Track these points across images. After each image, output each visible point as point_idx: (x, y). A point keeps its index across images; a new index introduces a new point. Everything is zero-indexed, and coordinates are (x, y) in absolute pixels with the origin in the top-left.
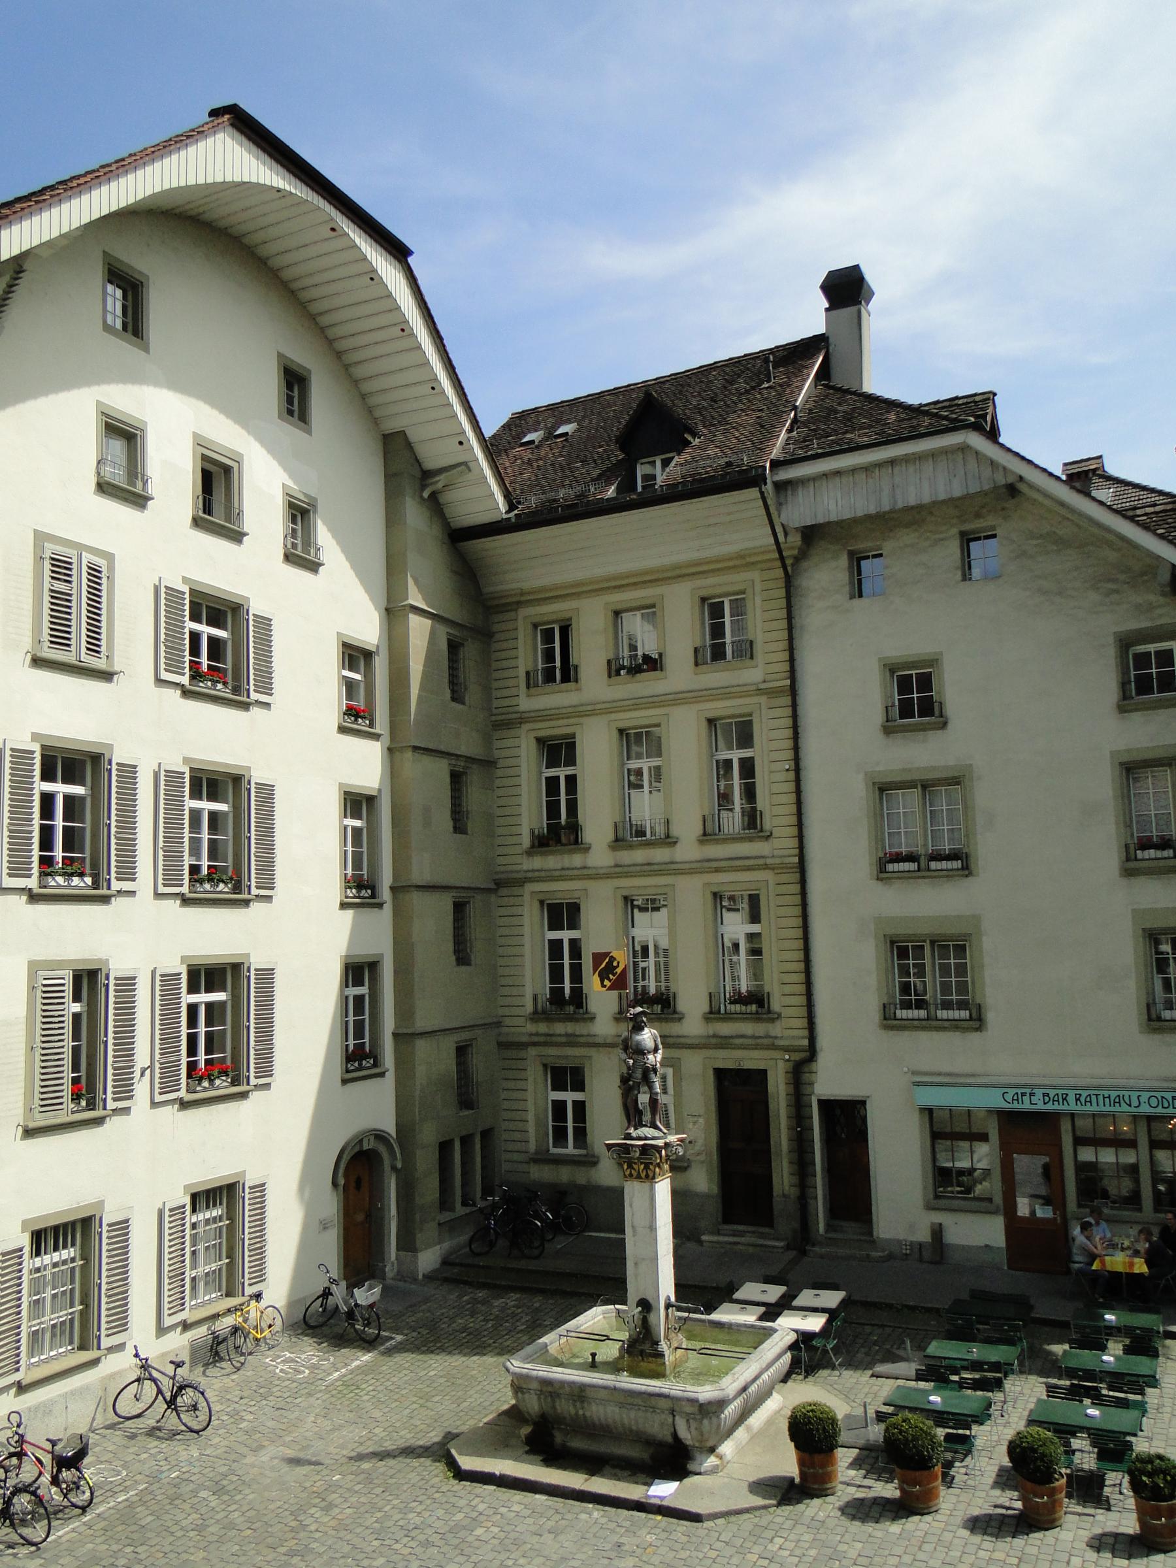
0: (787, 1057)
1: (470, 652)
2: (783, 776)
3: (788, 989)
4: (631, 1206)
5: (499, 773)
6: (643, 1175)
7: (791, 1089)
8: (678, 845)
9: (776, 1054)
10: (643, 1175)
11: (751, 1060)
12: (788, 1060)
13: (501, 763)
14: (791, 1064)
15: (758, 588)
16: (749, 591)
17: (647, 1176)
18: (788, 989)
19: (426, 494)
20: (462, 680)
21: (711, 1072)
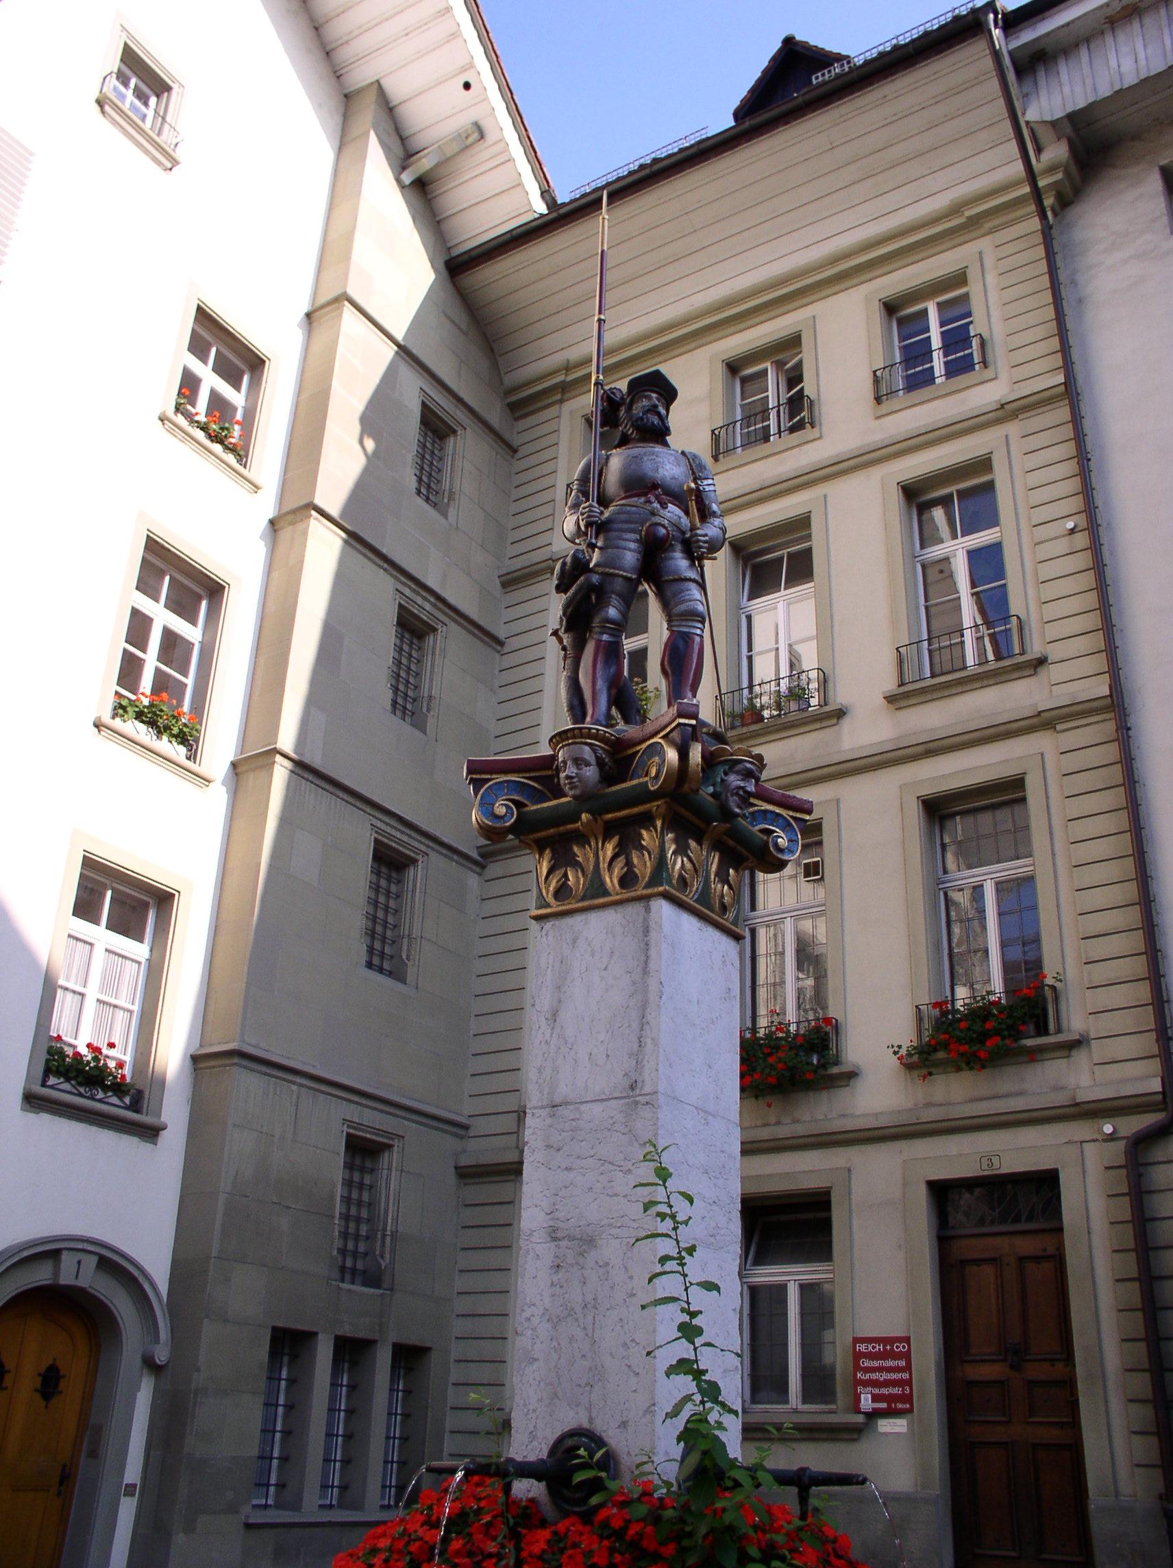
0: (1108, 1129)
1: (468, 453)
2: (1062, 546)
3: (1101, 948)
4: (554, 1016)
5: (508, 661)
6: (611, 881)
7: (1124, 1208)
8: (846, 723)
9: (1079, 1130)
10: (611, 881)
11: (1016, 1152)
12: (1111, 1138)
13: (512, 644)
14: (1121, 1145)
15: (989, 261)
16: (973, 275)
17: (627, 880)
18: (1101, 973)
19: (407, 178)
20: (446, 485)
21: (923, 1190)
